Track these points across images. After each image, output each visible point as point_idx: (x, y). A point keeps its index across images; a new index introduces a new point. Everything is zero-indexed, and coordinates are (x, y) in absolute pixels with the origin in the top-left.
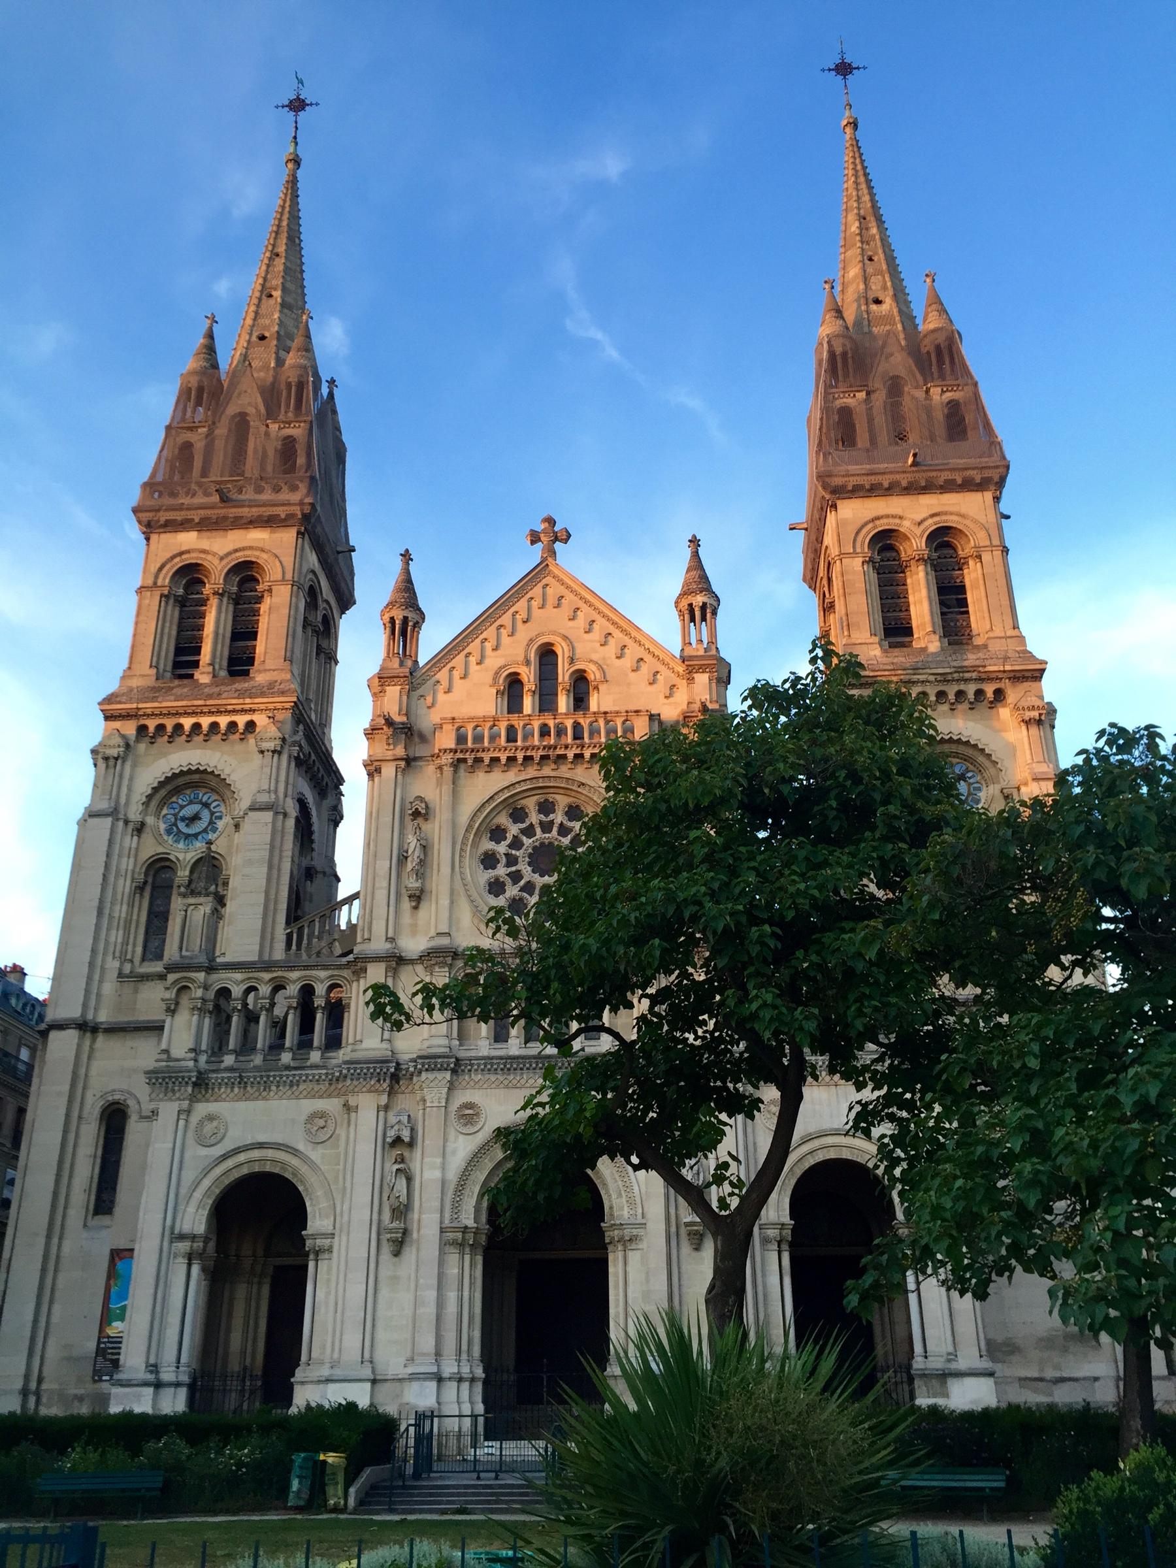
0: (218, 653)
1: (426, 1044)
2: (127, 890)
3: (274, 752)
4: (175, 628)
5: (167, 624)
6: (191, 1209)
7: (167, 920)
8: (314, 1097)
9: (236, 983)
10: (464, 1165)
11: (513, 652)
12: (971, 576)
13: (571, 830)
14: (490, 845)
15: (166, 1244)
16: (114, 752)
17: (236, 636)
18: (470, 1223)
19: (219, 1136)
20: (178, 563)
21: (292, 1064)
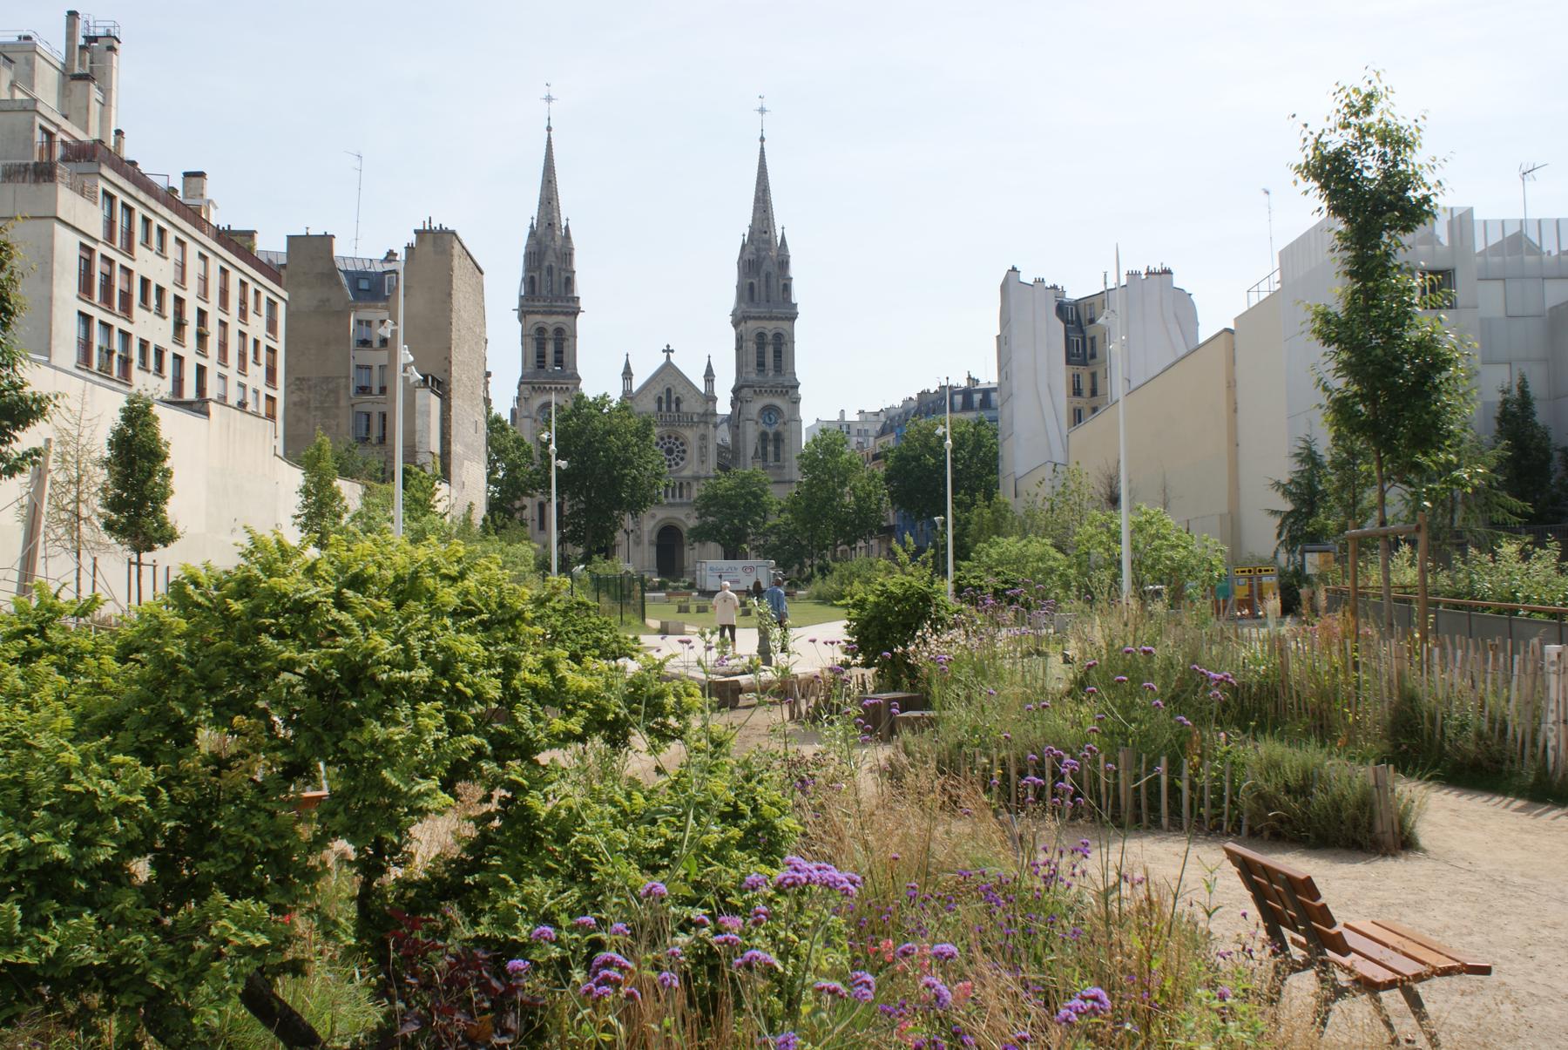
11: (659, 390)
12: (784, 349)
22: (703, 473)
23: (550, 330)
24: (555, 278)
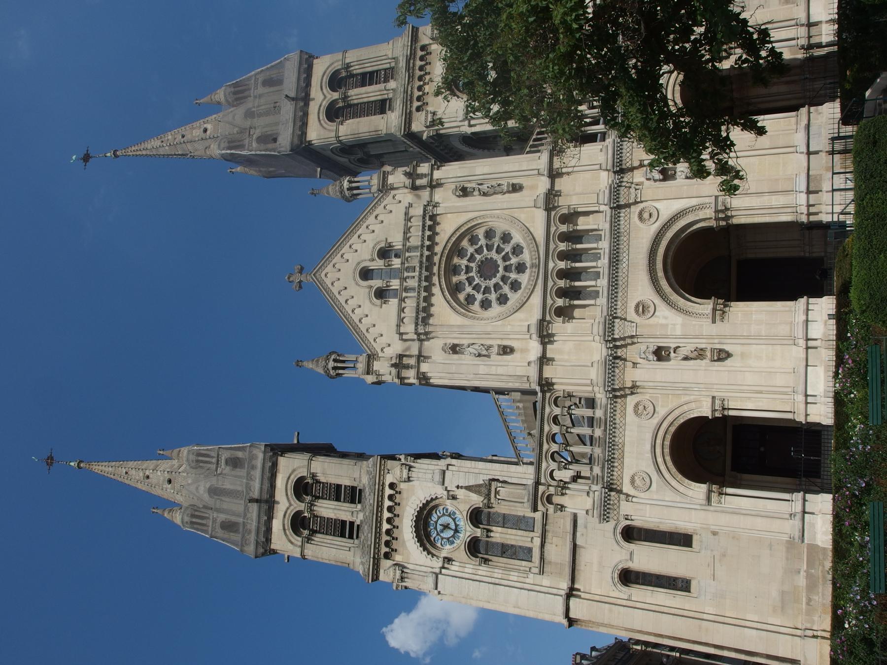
2: (485, 569)
3: (409, 470)
4: (328, 537)
6: (690, 493)
7: (507, 545)
8: (625, 414)
10: (674, 311)
13: (472, 255)
14: (477, 303)
16: (398, 573)
17: (338, 499)
18: (711, 306)
19: (645, 476)
20: (290, 532)
21: (602, 428)
22: (544, 184)
24: (228, 486)
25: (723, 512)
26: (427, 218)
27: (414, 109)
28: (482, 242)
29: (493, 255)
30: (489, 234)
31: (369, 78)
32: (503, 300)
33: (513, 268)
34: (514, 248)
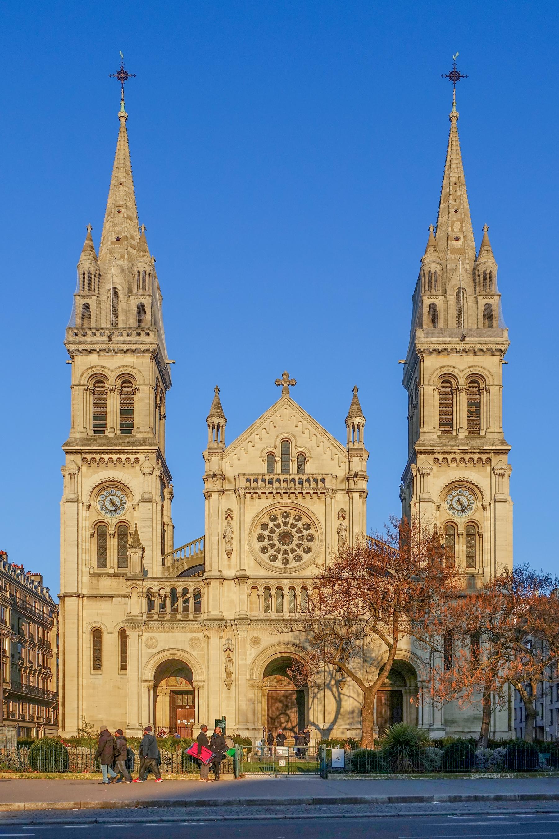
0: (115, 421)
1: (237, 614)
4: (91, 406)
5: (88, 405)
9: (155, 586)
14: (262, 531)
15: (139, 683)
16: (73, 471)
17: (123, 412)
18: (257, 679)
23: (112, 377)
25: (138, 689)
26: (323, 491)
27: (437, 456)
28: (305, 533)
29: (296, 541)
30: (311, 539)
31: (475, 408)
32: (264, 550)
33: (286, 556)
34: (299, 556)
